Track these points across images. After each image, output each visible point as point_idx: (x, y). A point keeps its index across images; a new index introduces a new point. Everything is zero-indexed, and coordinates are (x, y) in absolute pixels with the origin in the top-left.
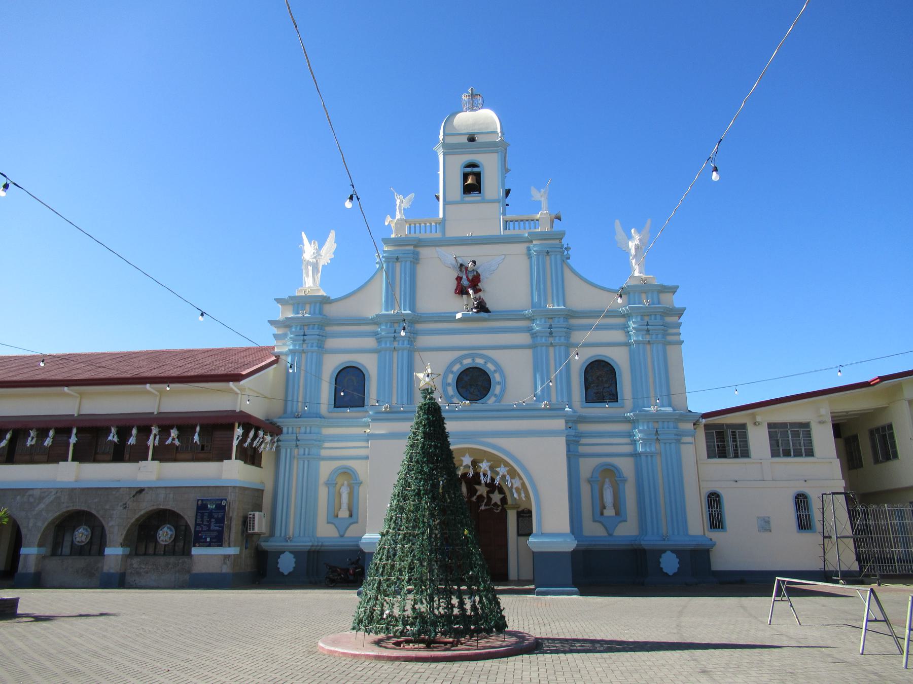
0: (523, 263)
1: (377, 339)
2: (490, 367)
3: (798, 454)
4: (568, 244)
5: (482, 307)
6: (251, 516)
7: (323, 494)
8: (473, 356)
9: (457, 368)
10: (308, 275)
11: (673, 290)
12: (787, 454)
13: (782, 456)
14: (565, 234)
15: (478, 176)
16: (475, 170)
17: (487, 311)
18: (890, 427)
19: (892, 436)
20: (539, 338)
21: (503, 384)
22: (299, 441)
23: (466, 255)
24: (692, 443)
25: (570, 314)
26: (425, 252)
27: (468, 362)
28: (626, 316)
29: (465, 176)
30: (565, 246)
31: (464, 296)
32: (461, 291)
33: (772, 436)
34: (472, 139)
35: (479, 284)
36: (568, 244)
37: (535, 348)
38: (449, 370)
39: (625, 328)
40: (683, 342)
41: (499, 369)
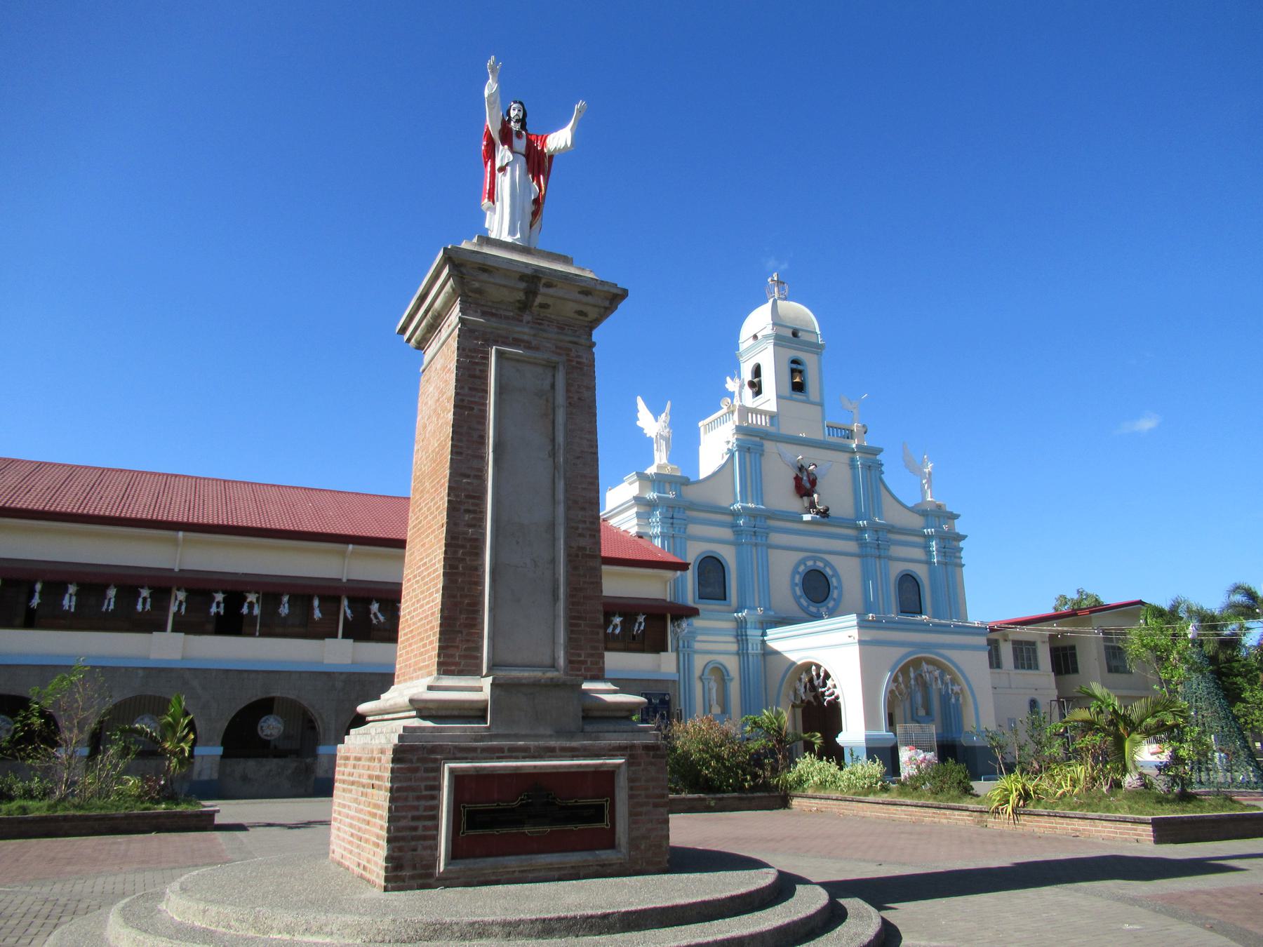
0: (846, 473)
2: (829, 571)
3: (1030, 668)
5: (825, 514)
6: (679, 711)
7: (698, 688)
8: (815, 559)
10: (659, 450)
12: (1023, 668)
13: (1020, 667)
18: (1073, 648)
19: (1074, 656)
20: (869, 549)
21: (840, 587)
23: (800, 455)
25: (891, 529)
26: (768, 445)
27: (810, 563)
28: (929, 538)
29: (793, 371)
31: (805, 498)
33: (1015, 650)
34: (795, 334)
38: (795, 571)
39: (927, 548)
40: (964, 565)
41: (836, 574)
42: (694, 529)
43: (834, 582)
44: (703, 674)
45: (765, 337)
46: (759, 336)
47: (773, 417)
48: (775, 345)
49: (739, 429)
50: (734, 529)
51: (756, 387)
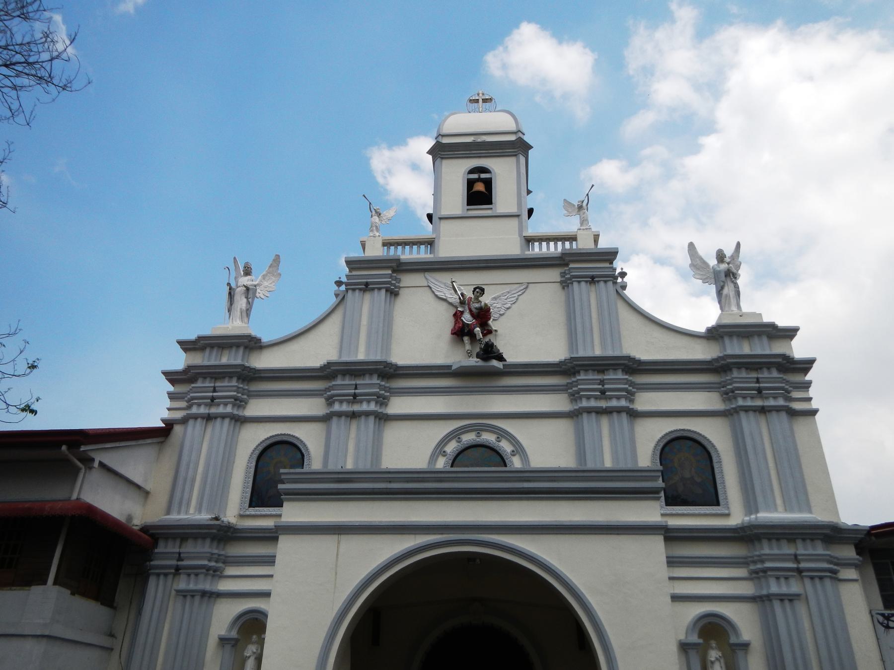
1: (327, 399)
2: (506, 447)
4: (622, 269)
9: (452, 447)
11: (790, 333)
14: (617, 253)
15: (488, 183)
16: (483, 176)
17: (500, 358)
22: (182, 560)
24: (855, 580)
25: (632, 366)
26: (408, 280)
27: (469, 438)
29: (470, 183)
30: (618, 271)
32: (461, 332)
35: (490, 322)
36: (622, 269)
37: (577, 416)
38: (439, 450)
41: (519, 449)
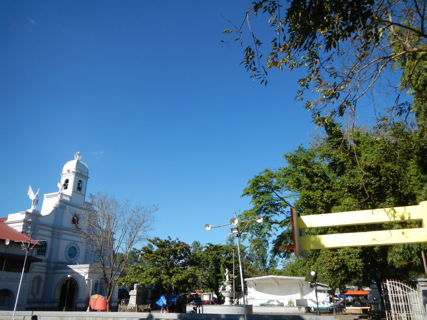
2: (77, 248)
26: (68, 207)
27: (72, 245)
29: (79, 184)
38: (67, 247)
41: (79, 249)
42: (40, 232)
43: (78, 251)
44: (33, 279)
45: (73, 172)
46: (71, 171)
47: (70, 197)
48: (75, 175)
49: (60, 201)
50: (52, 232)
51: (65, 186)
